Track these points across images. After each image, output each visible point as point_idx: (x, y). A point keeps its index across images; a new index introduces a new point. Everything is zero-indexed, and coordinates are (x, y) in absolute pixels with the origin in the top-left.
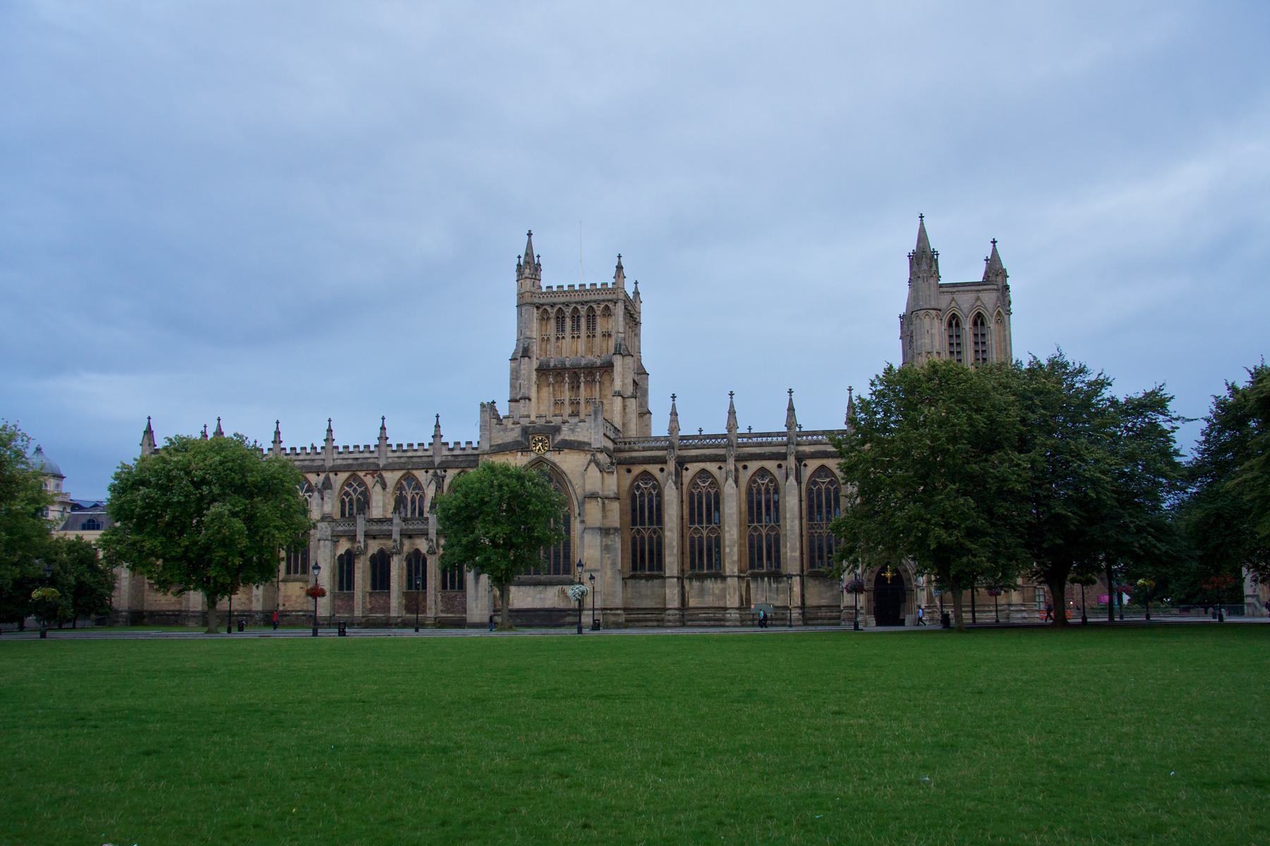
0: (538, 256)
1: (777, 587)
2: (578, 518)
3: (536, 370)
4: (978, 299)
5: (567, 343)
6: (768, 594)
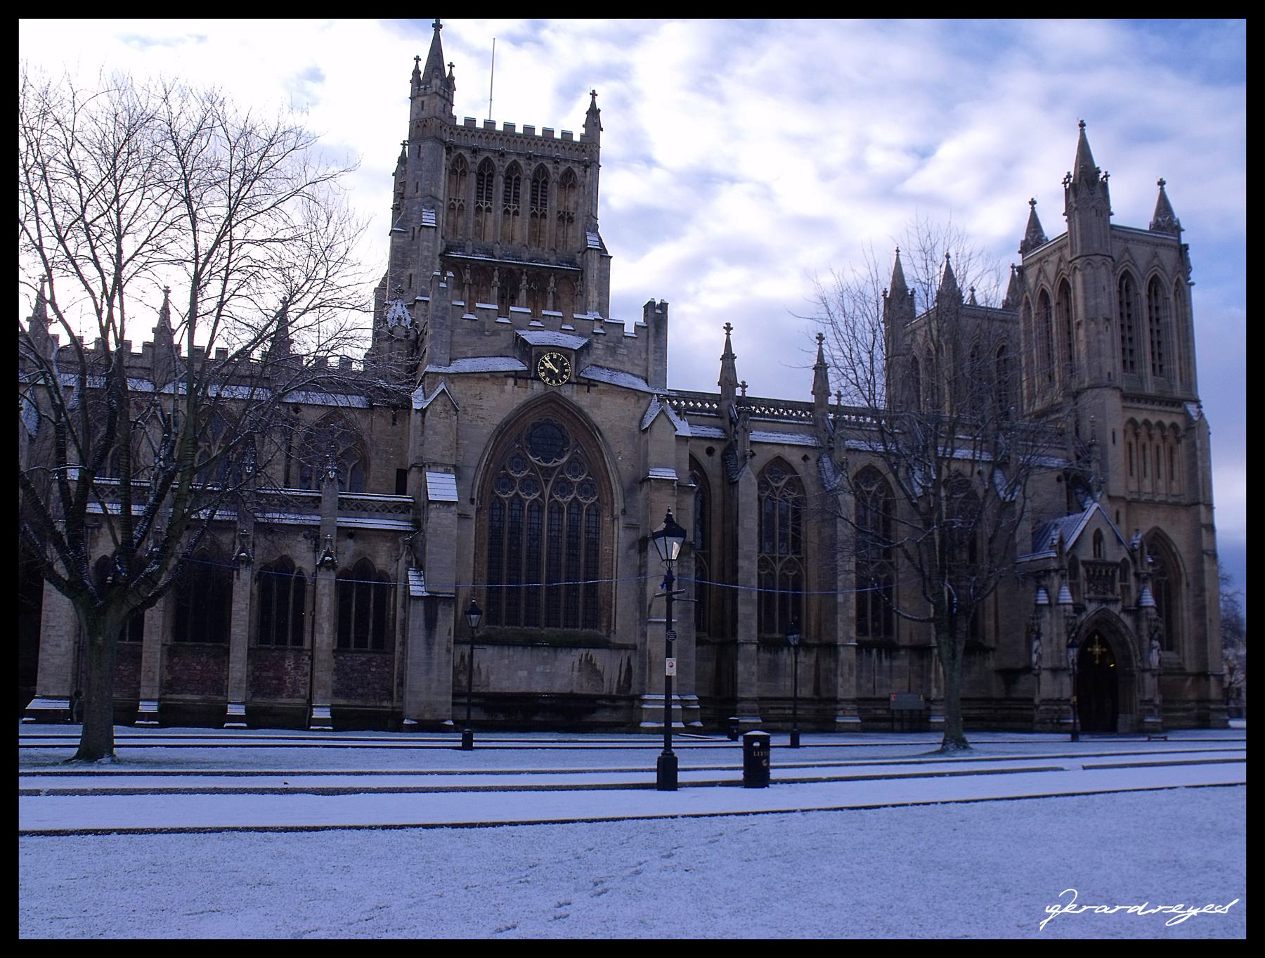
0: (451, 65)
1: (891, 666)
2: (621, 517)
3: (440, 255)
4: (1155, 255)
5: (493, 220)
6: (877, 677)
